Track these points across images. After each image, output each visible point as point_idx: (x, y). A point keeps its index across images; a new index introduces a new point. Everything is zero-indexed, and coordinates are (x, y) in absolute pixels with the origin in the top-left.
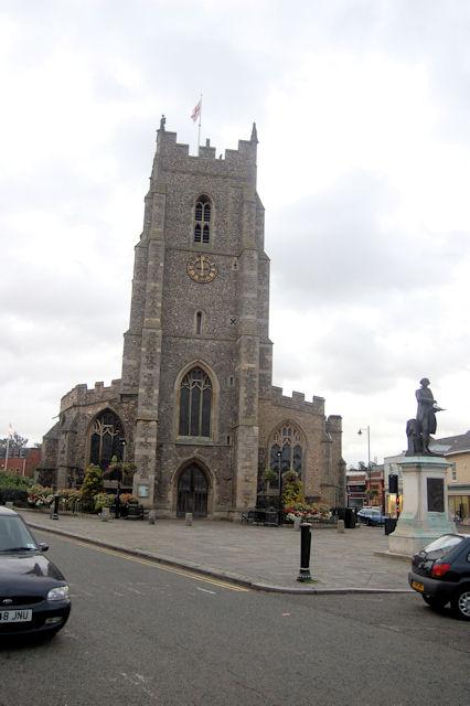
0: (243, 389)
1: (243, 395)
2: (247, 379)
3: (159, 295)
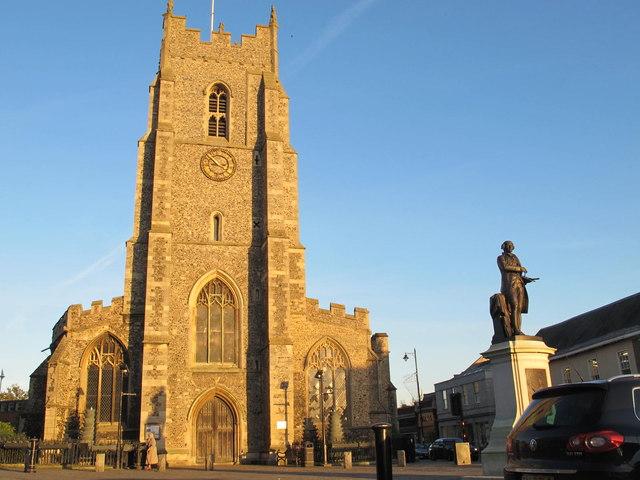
0: (271, 301)
1: (272, 309)
2: (276, 289)
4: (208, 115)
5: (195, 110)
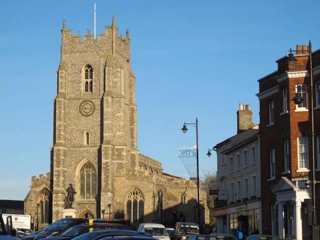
3: (62, 128)
4: (84, 80)
5: (77, 81)
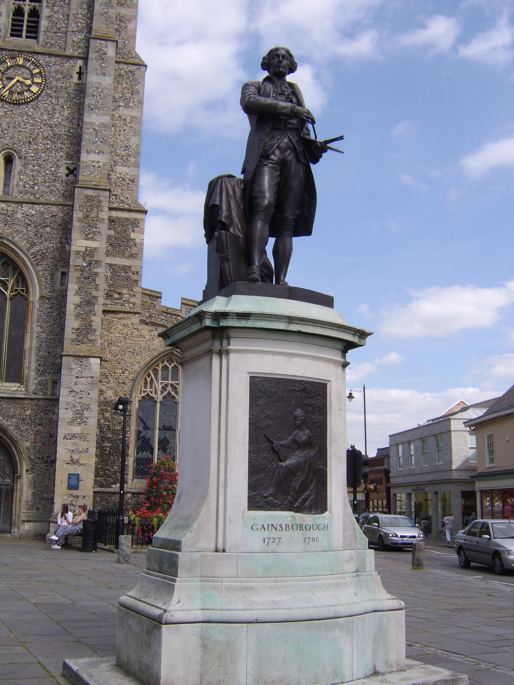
0: (72, 287)
2: (82, 269)
